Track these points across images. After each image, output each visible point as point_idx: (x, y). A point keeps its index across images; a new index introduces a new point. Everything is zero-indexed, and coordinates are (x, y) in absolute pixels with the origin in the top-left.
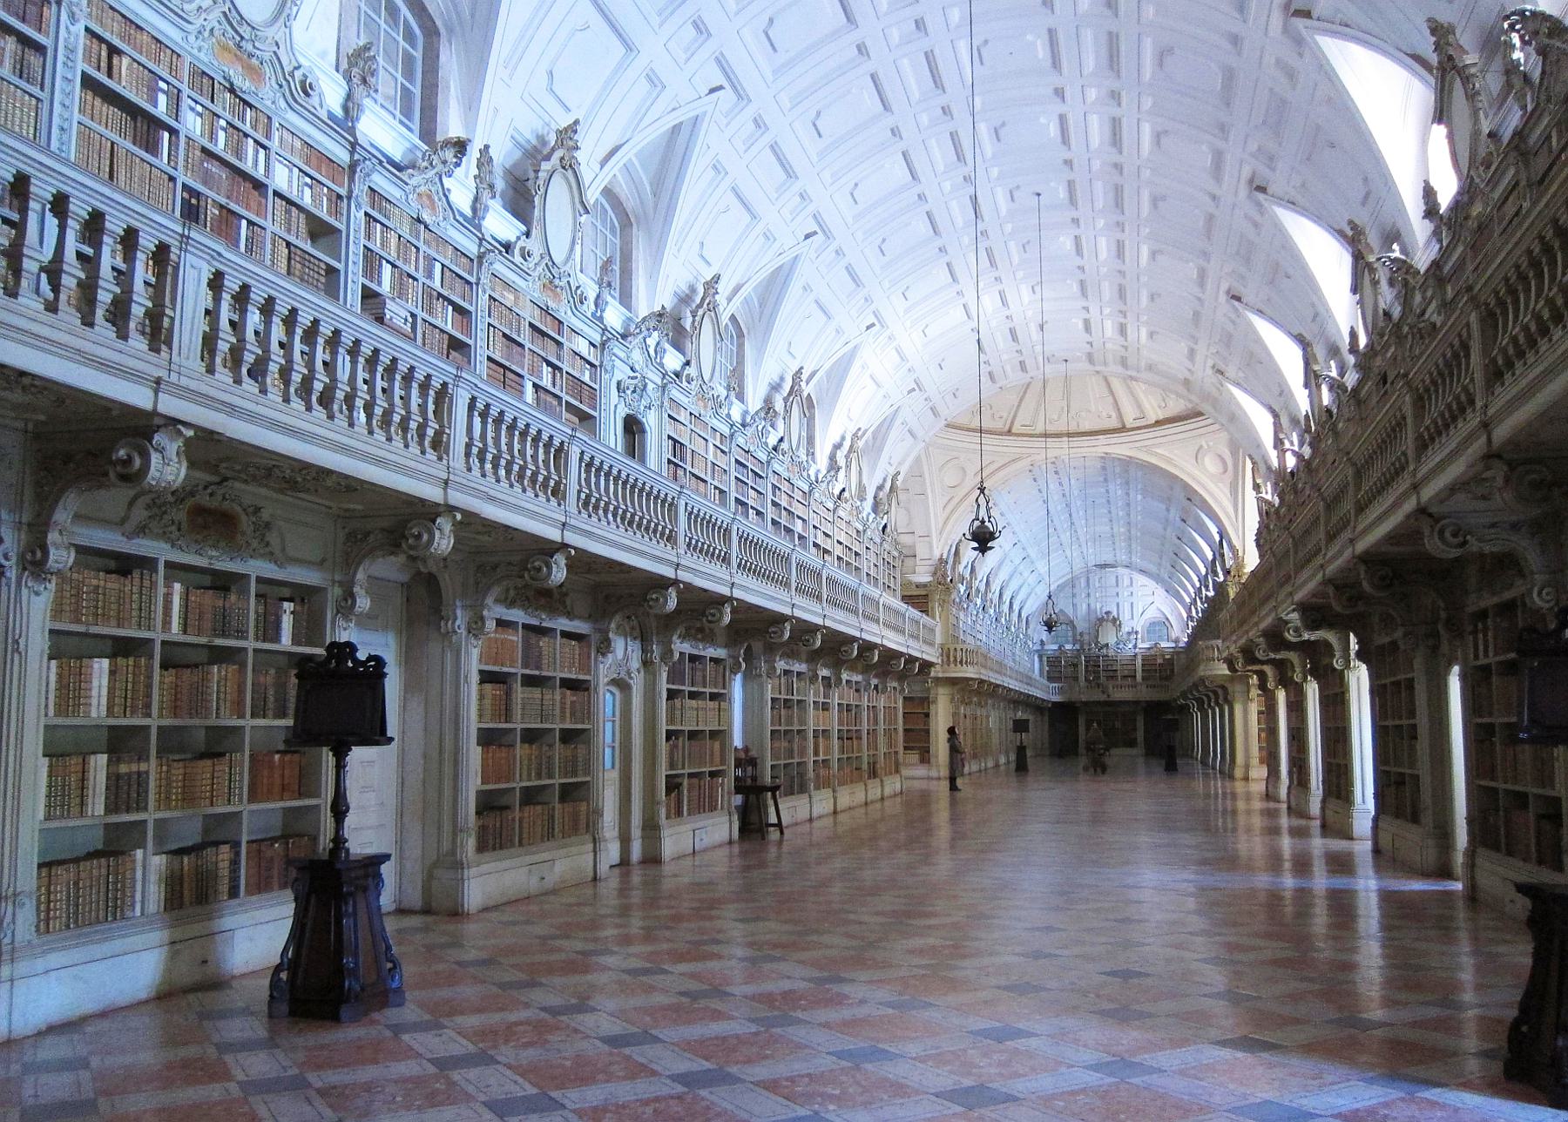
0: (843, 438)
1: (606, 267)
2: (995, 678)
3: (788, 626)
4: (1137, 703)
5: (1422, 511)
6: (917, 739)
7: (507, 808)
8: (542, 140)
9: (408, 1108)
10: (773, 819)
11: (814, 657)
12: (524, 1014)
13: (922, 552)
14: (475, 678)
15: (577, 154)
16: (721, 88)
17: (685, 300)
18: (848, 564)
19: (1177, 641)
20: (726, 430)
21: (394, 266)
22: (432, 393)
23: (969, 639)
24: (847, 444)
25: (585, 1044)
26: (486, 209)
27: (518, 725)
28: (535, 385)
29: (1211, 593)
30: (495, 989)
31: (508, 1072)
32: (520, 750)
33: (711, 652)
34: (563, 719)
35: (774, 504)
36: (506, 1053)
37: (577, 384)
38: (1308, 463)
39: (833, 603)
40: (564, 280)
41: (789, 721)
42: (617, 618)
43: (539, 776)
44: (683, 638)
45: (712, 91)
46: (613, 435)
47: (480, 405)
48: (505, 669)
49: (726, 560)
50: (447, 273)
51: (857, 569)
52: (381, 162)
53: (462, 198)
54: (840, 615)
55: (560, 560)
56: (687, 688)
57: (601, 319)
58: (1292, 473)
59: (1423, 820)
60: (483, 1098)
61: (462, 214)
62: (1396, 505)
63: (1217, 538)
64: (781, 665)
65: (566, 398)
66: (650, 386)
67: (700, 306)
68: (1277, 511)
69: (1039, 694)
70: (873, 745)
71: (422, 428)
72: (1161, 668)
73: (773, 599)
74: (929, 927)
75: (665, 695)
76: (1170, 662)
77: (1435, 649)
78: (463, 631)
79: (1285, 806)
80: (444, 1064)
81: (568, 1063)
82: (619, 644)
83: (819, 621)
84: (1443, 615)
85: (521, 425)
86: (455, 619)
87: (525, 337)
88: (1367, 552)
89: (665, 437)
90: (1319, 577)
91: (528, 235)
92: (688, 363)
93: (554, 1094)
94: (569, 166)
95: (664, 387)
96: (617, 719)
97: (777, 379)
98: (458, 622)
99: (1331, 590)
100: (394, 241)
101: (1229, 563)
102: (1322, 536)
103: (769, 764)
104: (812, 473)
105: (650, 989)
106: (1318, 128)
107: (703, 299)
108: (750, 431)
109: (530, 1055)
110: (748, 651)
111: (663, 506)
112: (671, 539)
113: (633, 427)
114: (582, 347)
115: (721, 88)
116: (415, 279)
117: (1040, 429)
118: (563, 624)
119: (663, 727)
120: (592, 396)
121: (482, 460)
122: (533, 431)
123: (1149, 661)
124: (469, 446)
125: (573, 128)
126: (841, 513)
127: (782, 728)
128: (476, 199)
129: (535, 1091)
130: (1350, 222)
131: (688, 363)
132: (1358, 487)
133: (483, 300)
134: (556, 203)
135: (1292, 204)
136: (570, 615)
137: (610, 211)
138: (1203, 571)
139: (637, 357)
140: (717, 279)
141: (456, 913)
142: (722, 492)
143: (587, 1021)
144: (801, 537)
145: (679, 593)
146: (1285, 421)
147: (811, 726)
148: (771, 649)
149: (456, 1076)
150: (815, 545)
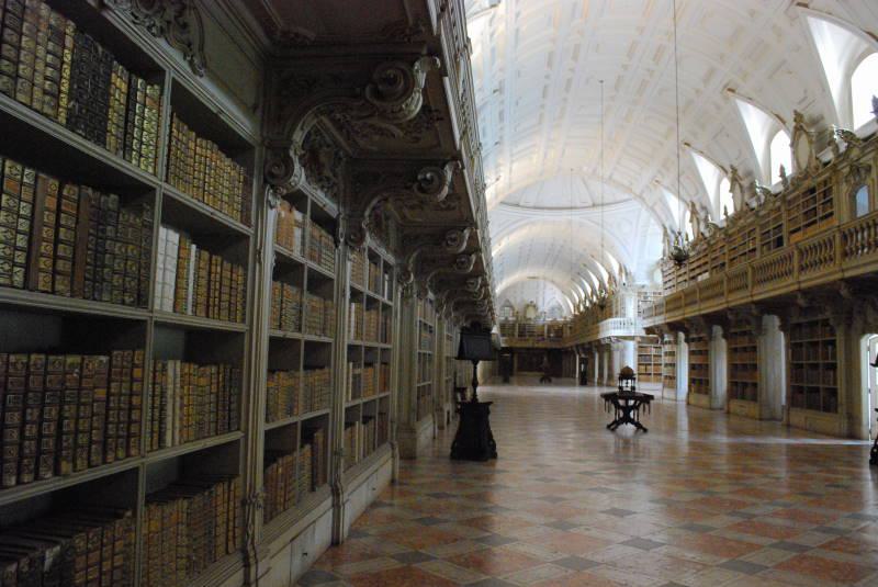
4: (545, 349)
19: (565, 318)
59: (839, 409)
72: (558, 330)
76: (561, 329)
77: (849, 326)
90: (796, 287)
117: (531, 204)
123: (550, 327)
135: (750, 100)
146: (698, 207)
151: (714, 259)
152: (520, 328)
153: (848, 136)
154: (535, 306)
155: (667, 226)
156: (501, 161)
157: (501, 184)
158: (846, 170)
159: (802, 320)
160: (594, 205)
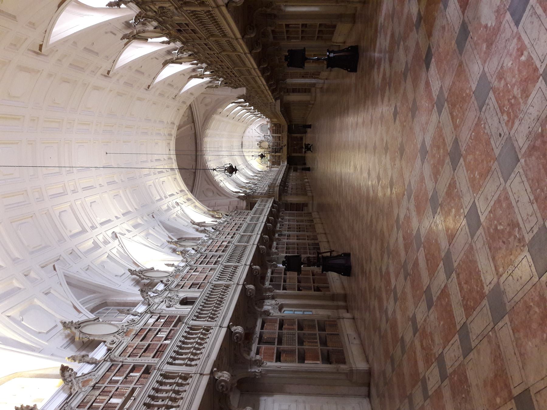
0: (194, 228)
1: (121, 312)
2: (279, 181)
3: (261, 246)
4: (288, 136)
5: (227, 5)
6: (299, 207)
7: (328, 351)
8: (67, 336)
9: (469, 392)
10: (329, 254)
11: (271, 240)
12: (417, 343)
13: (236, 204)
14: (279, 364)
15: (74, 322)
16: (54, 266)
17: (137, 283)
18: (239, 227)
19: (268, 122)
20: (188, 268)
21: (111, 397)
22: (164, 380)
23: (266, 188)
24: (197, 227)
25: (432, 317)
26: (92, 358)
27: (297, 347)
28: (165, 340)
29: (252, 107)
30: (405, 356)
31: (447, 348)
32: (306, 346)
33: (269, 274)
34: (293, 329)
35: (216, 251)
36: (437, 350)
37: (165, 324)
38: (208, 64)
39: (252, 231)
40: (124, 327)
41: (294, 248)
42: (256, 308)
43: (316, 339)
44: (264, 284)
45: (55, 269)
46: (187, 309)
47: (171, 360)
48: (275, 352)
49: (236, 267)
50: (117, 374)
51: (241, 224)
52: (67, 403)
53: (88, 368)
54: (257, 229)
55: (233, 329)
56: (282, 283)
57: (141, 314)
58: (212, 72)
60: (461, 358)
61: (93, 369)
62: (224, 17)
63: (234, 104)
64: (274, 250)
65: (171, 327)
66: (169, 295)
67: (140, 276)
68: (225, 79)
69: (284, 168)
70: (302, 221)
71: (179, 385)
72: (276, 129)
73: (251, 251)
74: (373, 191)
75: (284, 291)
76: (275, 125)
78: (260, 369)
79: (326, 81)
80: (443, 376)
81: (442, 323)
82: (266, 308)
83: (259, 236)
84: (264, 8)
85: (180, 344)
86: (255, 371)
87: (146, 343)
88: (241, 33)
89: (189, 290)
90: (249, 55)
91: (105, 342)
92: (162, 281)
93: (458, 328)
94: (79, 325)
95: (170, 290)
96: (293, 309)
97: (171, 250)
98: (257, 371)
99: (254, 51)
100: (101, 397)
101: (242, 100)
102: (233, 54)
103: (309, 255)
104: (206, 238)
105: (403, 293)
106: (85, 48)
107: (137, 275)
108: (189, 260)
109: (438, 340)
110: (269, 261)
111: (215, 290)
112: (227, 287)
113: (185, 302)
114: (152, 321)
115: (54, 266)
116: (118, 388)
117: (194, 163)
118: (258, 329)
119: (296, 292)
120: (171, 317)
121: (193, 360)
122: (183, 339)
124: (187, 365)
125: (64, 324)
126: (221, 229)
127: (296, 251)
128: (88, 363)
129: (457, 336)
130: (121, 39)
131: (162, 281)
132: (217, 36)
133: (130, 360)
134: (94, 331)
136: (255, 326)
137: (100, 310)
138: (245, 110)
139: (157, 300)
140: (130, 270)
141: (369, 373)
142: (211, 270)
143: (420, 318)
144: (229, 243)
145: (248, 284)
146: (194, 74)
147: (295, 241)
148: (269, 254)
149: (449, 371)
150: (232, 238)
151: (228, 68)
152: (274, 153)
153: (137, 17)
154: (260, 142)
155: (207, 86)
156: (165, 207)
157: (181, 199)
158: (164, 18)
159: (271, 36)
160: (193, 122)
